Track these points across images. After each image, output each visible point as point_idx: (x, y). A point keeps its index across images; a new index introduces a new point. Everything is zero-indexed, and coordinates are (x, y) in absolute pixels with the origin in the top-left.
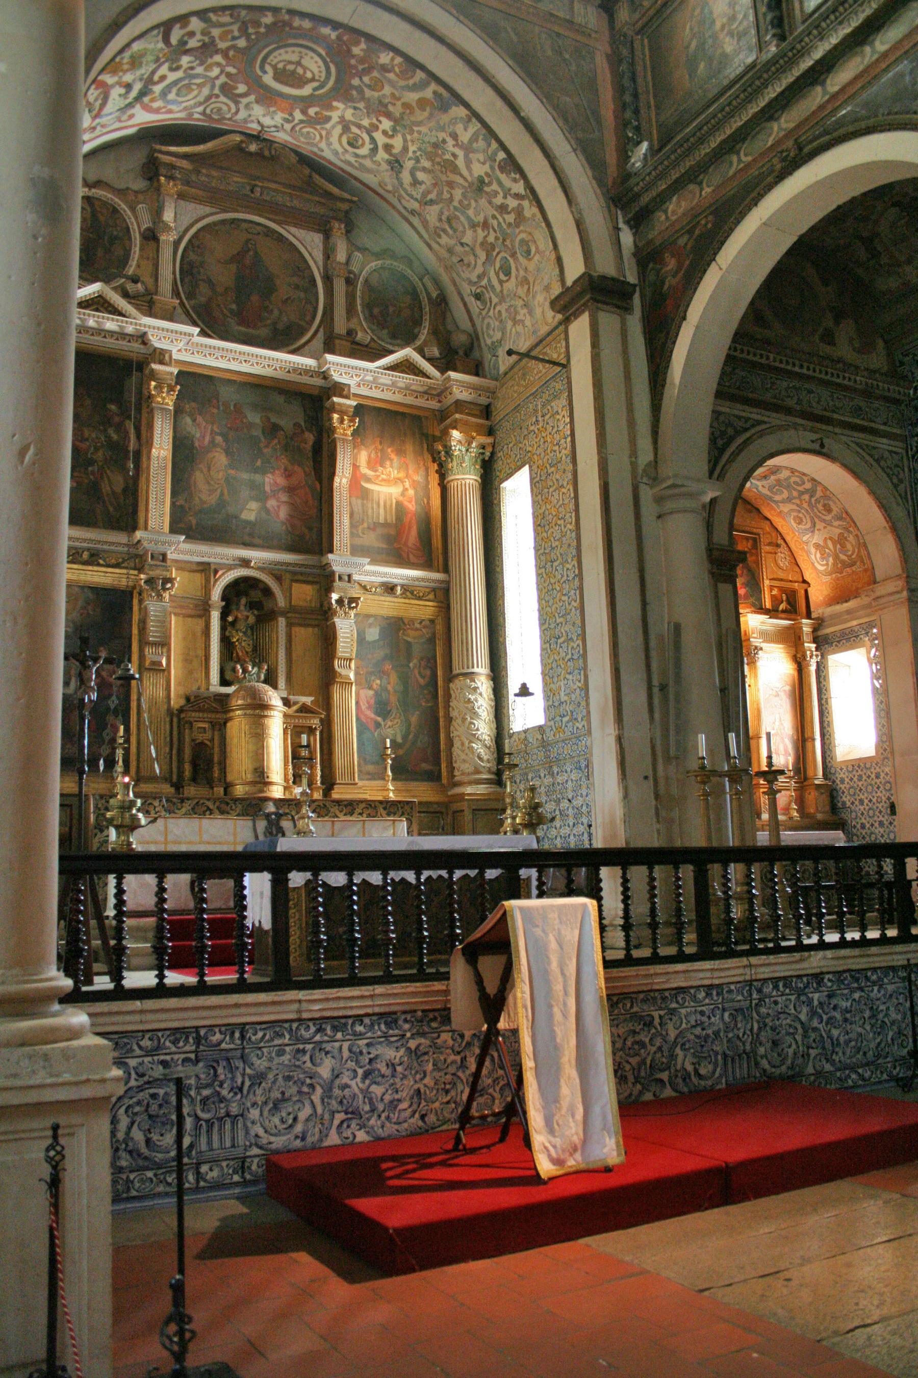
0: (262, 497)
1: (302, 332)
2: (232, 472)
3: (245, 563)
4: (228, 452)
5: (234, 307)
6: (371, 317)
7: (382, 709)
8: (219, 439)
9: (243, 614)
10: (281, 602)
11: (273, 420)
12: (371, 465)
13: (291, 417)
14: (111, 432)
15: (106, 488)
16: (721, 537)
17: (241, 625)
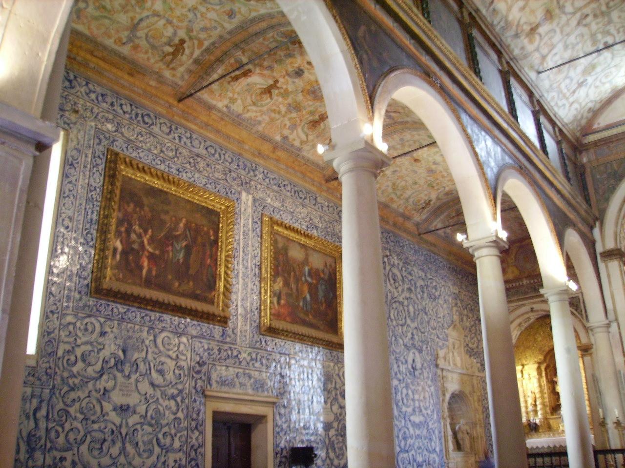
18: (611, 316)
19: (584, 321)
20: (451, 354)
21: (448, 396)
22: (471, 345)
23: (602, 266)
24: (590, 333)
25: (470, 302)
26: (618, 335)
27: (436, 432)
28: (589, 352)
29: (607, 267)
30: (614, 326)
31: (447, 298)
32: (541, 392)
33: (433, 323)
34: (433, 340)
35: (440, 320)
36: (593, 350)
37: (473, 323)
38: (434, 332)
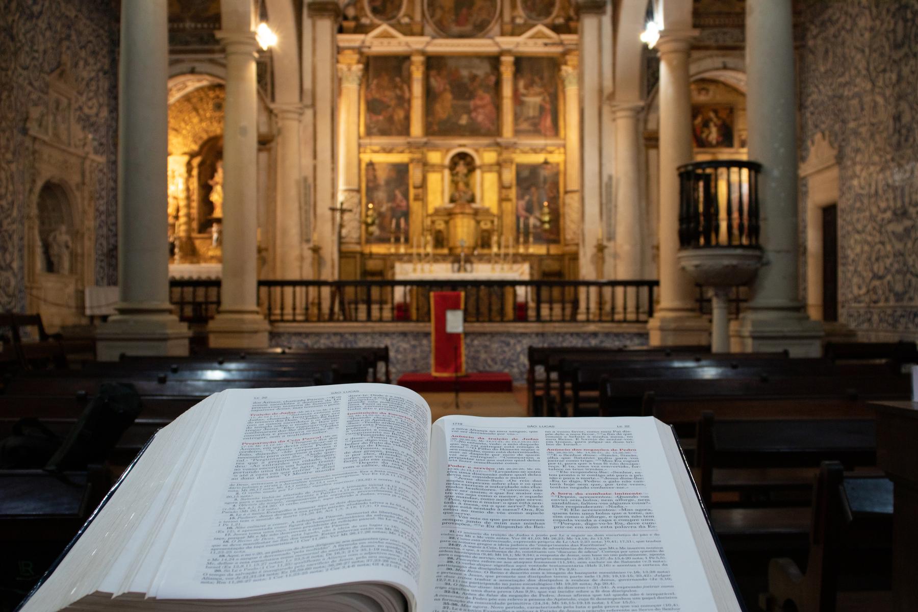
0: (469, 112)
1: (489, 23)
2: (455, 102)
3: (461, 146)
4: (452, 92)
5: (453, 17)
6: (526, 7)
7: (529, 209)
8: (448, 87)
9: (462, 168)
10: (478, 162)
11: (475, 72)
12: (527, 87)
13: (482, 70)
14: (398, 92)
15: (396, 118)
16: (651, 126)
17: (460, 175)
18: (308, 100)
19: (268, 100)
20: (51, 118)
21: (40, 184)
22: (86, 110)
23: (307, 22)
24: (273, 118)
25: (91, 38)
26: (311, 129)
27: (15, 237)
28: (268, 146)
29: (314, 26)
30: (309, 113)
31: (53, 21)
32: (188, 198)
33: (24, 59)
34: (21, 87)
35: (36, 55)
36: (273, 144)
37: (93, 74)
38: (25, 73)
